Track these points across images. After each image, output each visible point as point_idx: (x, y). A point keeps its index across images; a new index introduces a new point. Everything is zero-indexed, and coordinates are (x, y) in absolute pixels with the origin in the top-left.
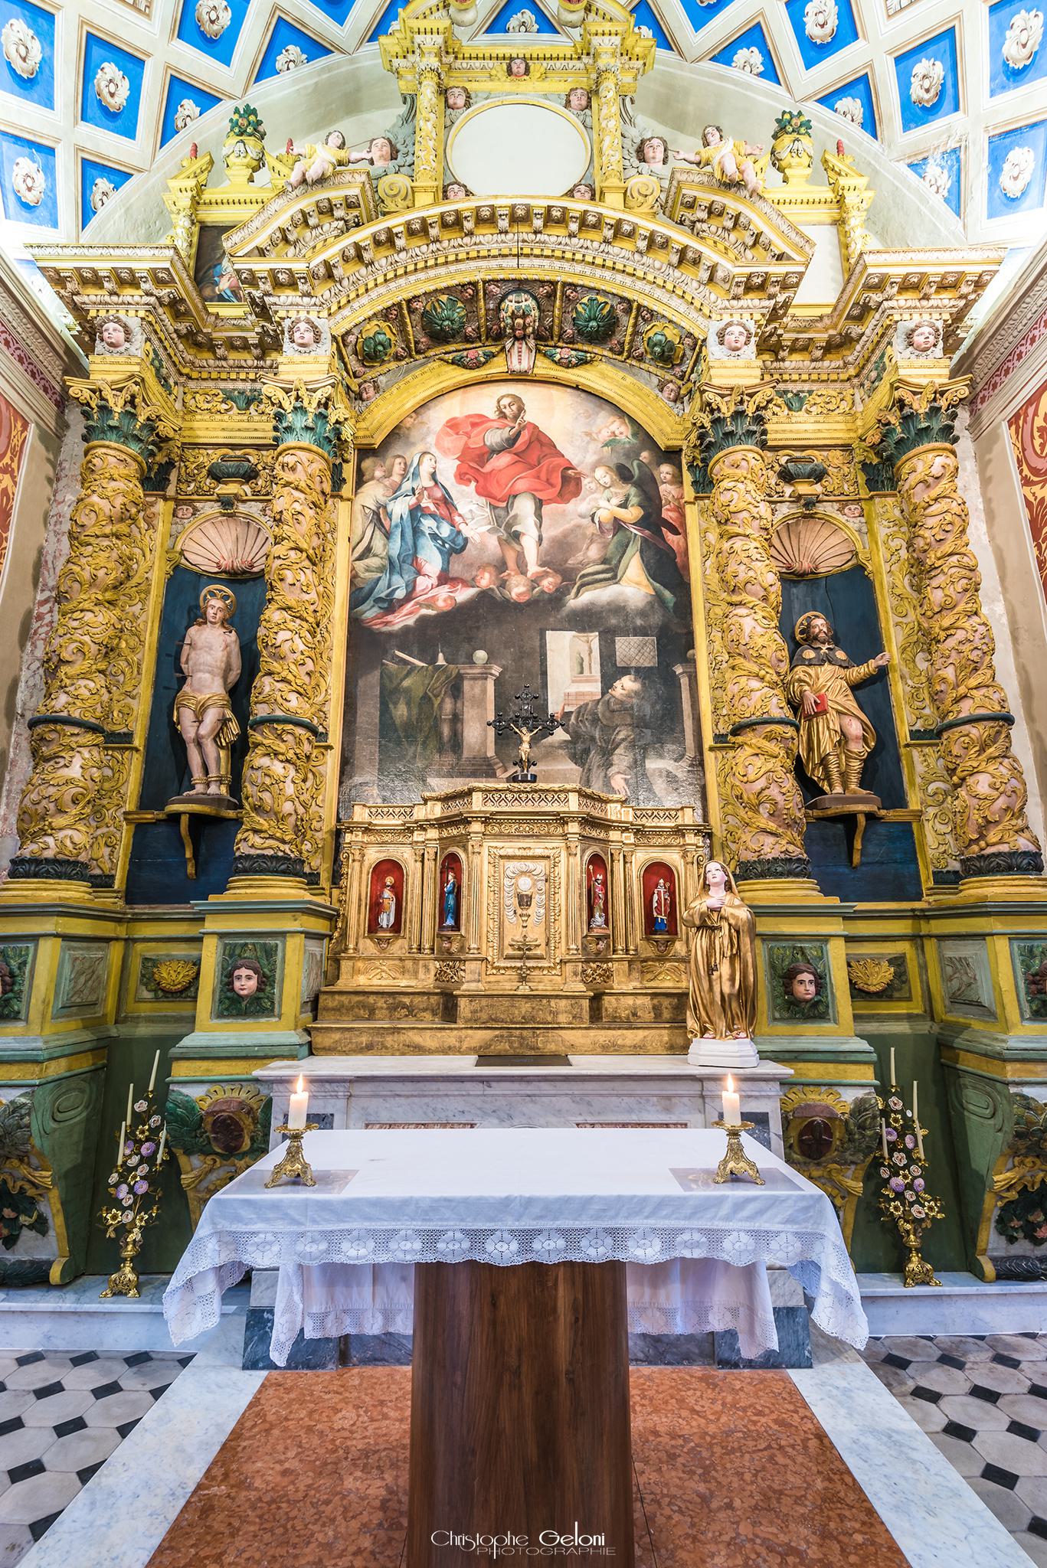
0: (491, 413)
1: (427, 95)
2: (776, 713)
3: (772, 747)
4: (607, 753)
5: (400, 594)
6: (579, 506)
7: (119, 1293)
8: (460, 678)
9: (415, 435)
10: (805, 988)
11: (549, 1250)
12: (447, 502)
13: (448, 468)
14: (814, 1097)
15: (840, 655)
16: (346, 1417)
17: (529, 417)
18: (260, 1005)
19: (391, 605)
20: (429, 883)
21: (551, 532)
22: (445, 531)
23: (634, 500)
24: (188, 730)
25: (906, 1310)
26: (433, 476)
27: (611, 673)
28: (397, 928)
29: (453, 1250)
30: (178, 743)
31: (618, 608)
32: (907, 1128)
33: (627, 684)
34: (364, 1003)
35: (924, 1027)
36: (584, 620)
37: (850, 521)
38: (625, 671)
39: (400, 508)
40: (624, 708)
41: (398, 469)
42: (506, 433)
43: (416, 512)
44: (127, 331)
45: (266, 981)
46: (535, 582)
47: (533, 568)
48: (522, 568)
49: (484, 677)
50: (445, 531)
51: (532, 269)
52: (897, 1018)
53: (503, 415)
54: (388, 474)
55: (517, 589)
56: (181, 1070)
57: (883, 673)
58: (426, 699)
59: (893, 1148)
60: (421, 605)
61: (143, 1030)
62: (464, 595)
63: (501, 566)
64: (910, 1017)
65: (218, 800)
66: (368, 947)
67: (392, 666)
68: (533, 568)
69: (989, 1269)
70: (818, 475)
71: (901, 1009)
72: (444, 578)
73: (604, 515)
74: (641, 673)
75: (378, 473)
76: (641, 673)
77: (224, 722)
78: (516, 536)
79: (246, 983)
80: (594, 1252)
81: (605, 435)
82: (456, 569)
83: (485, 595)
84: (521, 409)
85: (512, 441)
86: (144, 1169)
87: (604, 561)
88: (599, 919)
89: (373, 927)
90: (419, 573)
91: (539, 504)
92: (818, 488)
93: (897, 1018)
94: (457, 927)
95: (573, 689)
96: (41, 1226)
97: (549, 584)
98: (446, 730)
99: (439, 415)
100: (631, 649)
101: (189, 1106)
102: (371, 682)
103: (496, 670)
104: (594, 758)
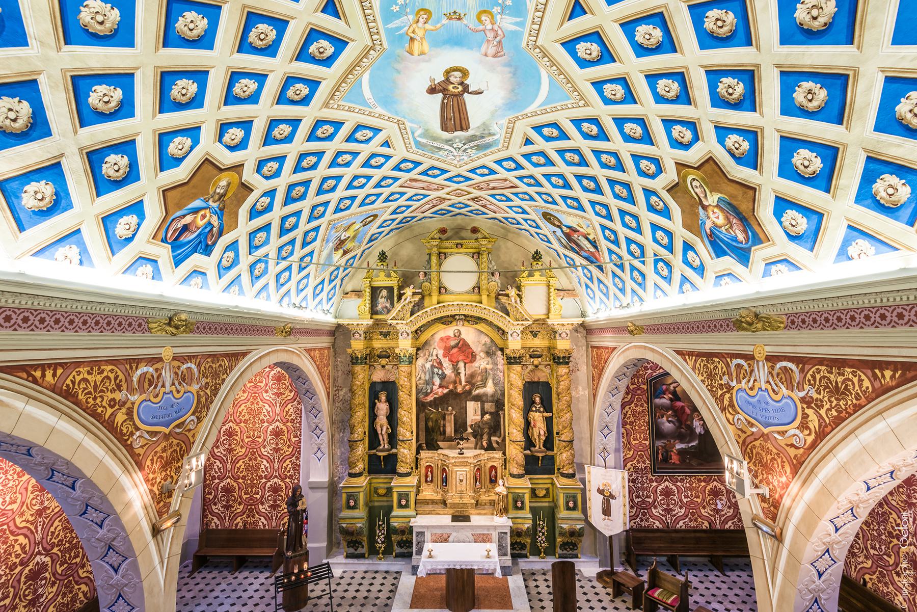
0: (452, 335)
1: (434, 260)
2: (519, 440)
3: (517, 447)
4: (482, 436)
5: (429, 391)
6: (476, 364)
7: (380, 559)
8: (445, 415)
9: (432, 342)
10: (519, 504)
11: (464, 567)
12: (440, 363)
13: (441, 353)
14: (519, 526)
15: (542, 409)
16: (432, 584)
17: (462, 336)
18: (407, 506)
19: (427, 394)
20: (439, 475)
21: (468, 372)
22: (440, 372)
23: (490, 362)
24: (379, 432)
25: (539, 564)
26: (437, 356)
27: (483, 413)
28: (431, 481)
29: (452, 567)
30: (375, 431)
31: (485, 395)
32: (543, 528)
33: (487, 417)
34: (426, 502)
35: (551, 504)
36: (477, 398)
37: (547, 370)
38: (487, 413)
39: (428, 365)
40: (486, 423)
41: (427, 353)
42: (456, 342)
43: (432, 366)
44: (360, 335)
45: (407, 501)
46: (464, 387)
47: (463, 383)
48: (460, 383)
49: (451, 414)
50: (440, 372)
51: (462, 312)
52: (546, 502)
53: (455, 336)
54: (425, 355)
55: (459, 389)
56: (392, 520)
57: (551, 417)
58: (436, 421)
59: (540, 532)
60: (434, 394)
61: (376, 504)
62: (446, 391)
63: (455, 382)
64: (549, 502)
65: (388, 450)
66: (425, 484)
67: (427, 411)
68: (463, 383)
69: (557, 556)
70: (540, 356)
71: (547, 500)
72: (441, 386)
73: (482, 367)
74: (491, 413)
75: (422, 355)
76: (491, 413)
77: (387, 428)
78: (459, 373)
79: (404, 502)
80: (469, 567)
81: (483, 342)
82: (444, 384)
83: (451, 391)
84: (460, 334)
85: (458, 344)
86: (383, 536)
87: (482, 380)
88: (478, 483)
89: (426, 481)
90: (434, 385)
91: (465, 364)
92: (540, 359)
93: (546, 502)
94: (446, 486)
95: (474, 418)
96: (363, 547)
97: (467, 388)
98: (442, 429)
99: (437, 337)
100: (489, 406)
101: (395, 527)
102: (422, 415)
103: (454, 413)
104: (479, 437)
